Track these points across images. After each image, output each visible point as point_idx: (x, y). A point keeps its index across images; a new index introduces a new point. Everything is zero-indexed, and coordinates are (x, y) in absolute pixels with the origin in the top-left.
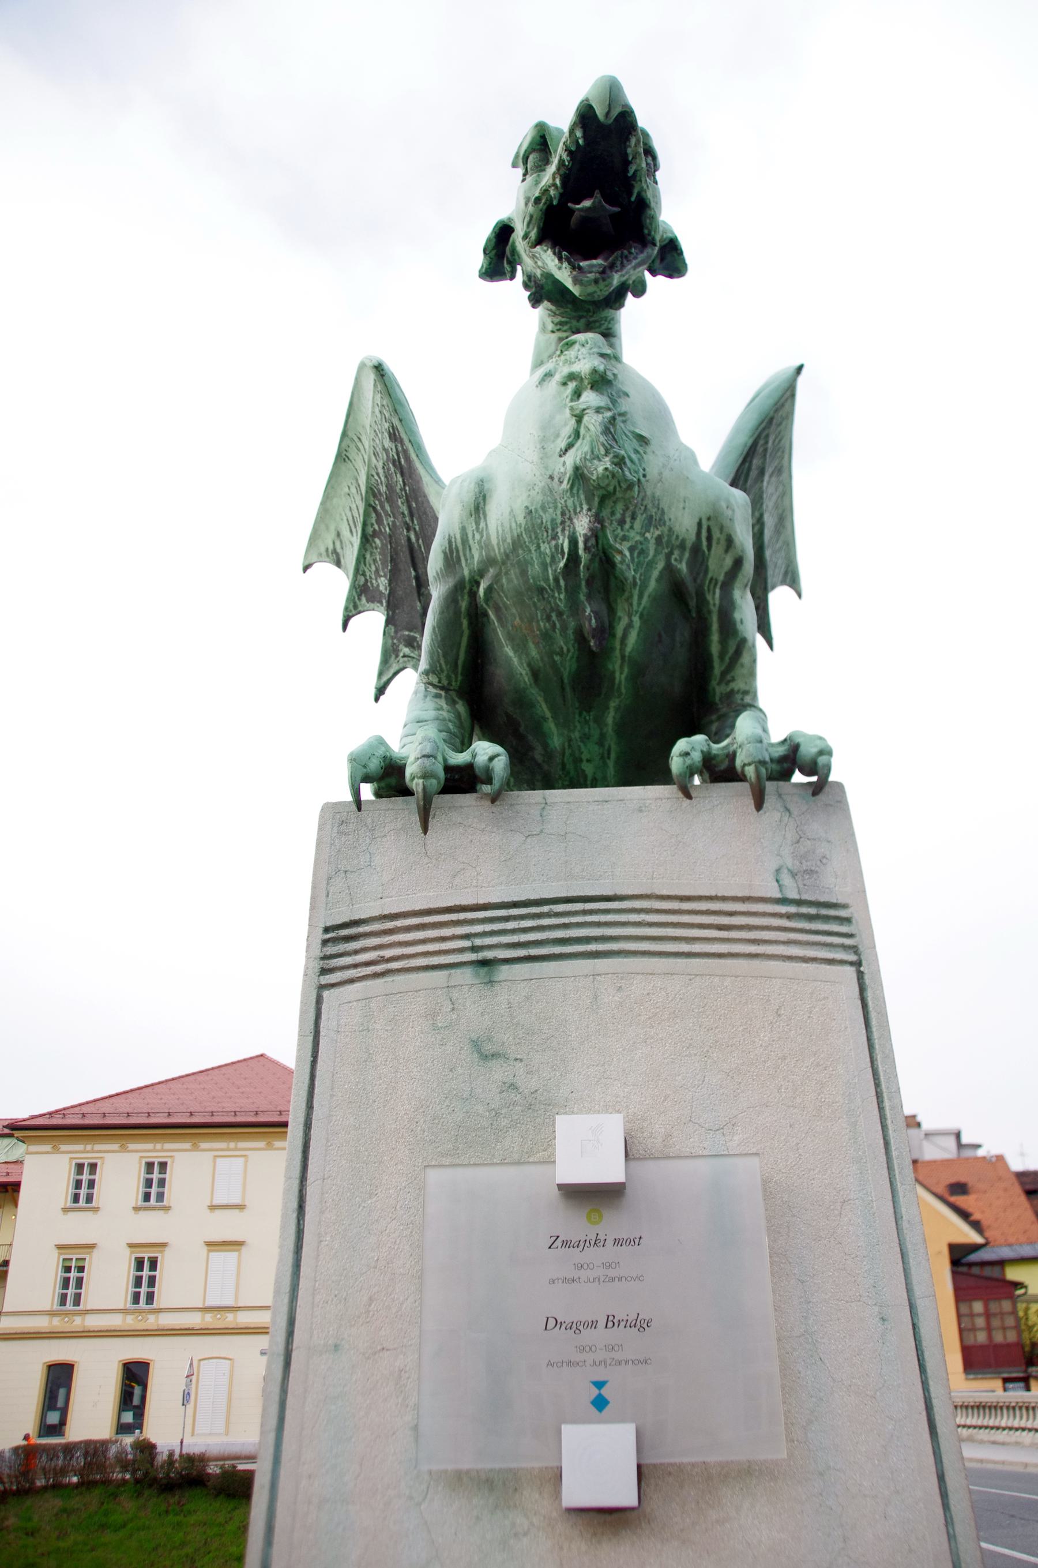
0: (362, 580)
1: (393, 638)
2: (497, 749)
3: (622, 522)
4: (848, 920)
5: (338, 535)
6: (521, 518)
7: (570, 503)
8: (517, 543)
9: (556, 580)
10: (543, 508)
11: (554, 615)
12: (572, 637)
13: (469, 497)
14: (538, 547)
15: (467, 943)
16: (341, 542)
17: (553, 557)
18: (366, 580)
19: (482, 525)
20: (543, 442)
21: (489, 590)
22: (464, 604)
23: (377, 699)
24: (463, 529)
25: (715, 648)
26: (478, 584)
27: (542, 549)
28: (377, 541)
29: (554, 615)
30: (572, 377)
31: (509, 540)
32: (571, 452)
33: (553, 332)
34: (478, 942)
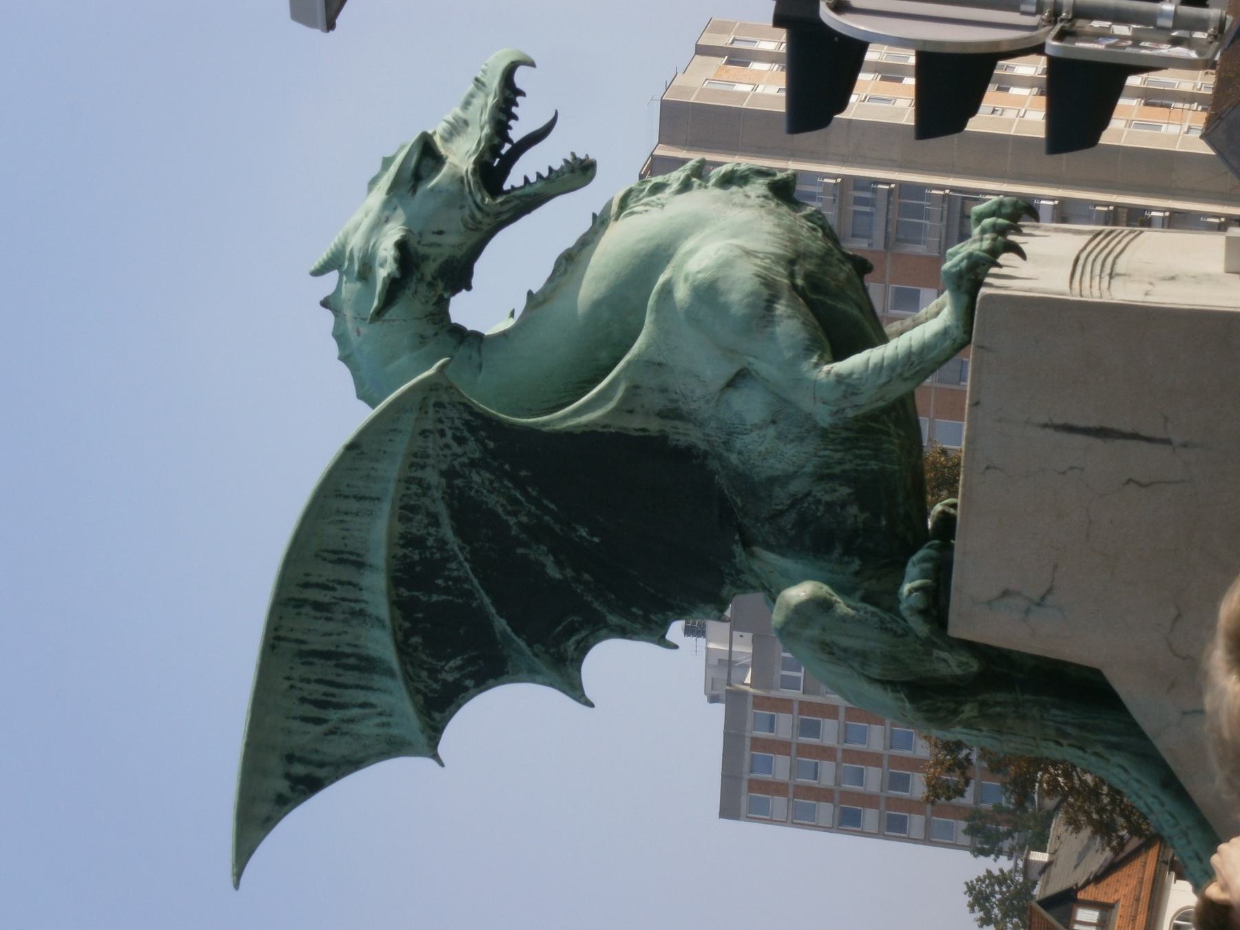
0: (420, 698)
1: (547, 652)
5: (290, 758)
6: (778, 230)
8: (794, 241)
15: (1097, 279)
16: (304, 761)
18: (425, 695)
23: (591, 705)
24: (756, 265)
28: (415, 640)
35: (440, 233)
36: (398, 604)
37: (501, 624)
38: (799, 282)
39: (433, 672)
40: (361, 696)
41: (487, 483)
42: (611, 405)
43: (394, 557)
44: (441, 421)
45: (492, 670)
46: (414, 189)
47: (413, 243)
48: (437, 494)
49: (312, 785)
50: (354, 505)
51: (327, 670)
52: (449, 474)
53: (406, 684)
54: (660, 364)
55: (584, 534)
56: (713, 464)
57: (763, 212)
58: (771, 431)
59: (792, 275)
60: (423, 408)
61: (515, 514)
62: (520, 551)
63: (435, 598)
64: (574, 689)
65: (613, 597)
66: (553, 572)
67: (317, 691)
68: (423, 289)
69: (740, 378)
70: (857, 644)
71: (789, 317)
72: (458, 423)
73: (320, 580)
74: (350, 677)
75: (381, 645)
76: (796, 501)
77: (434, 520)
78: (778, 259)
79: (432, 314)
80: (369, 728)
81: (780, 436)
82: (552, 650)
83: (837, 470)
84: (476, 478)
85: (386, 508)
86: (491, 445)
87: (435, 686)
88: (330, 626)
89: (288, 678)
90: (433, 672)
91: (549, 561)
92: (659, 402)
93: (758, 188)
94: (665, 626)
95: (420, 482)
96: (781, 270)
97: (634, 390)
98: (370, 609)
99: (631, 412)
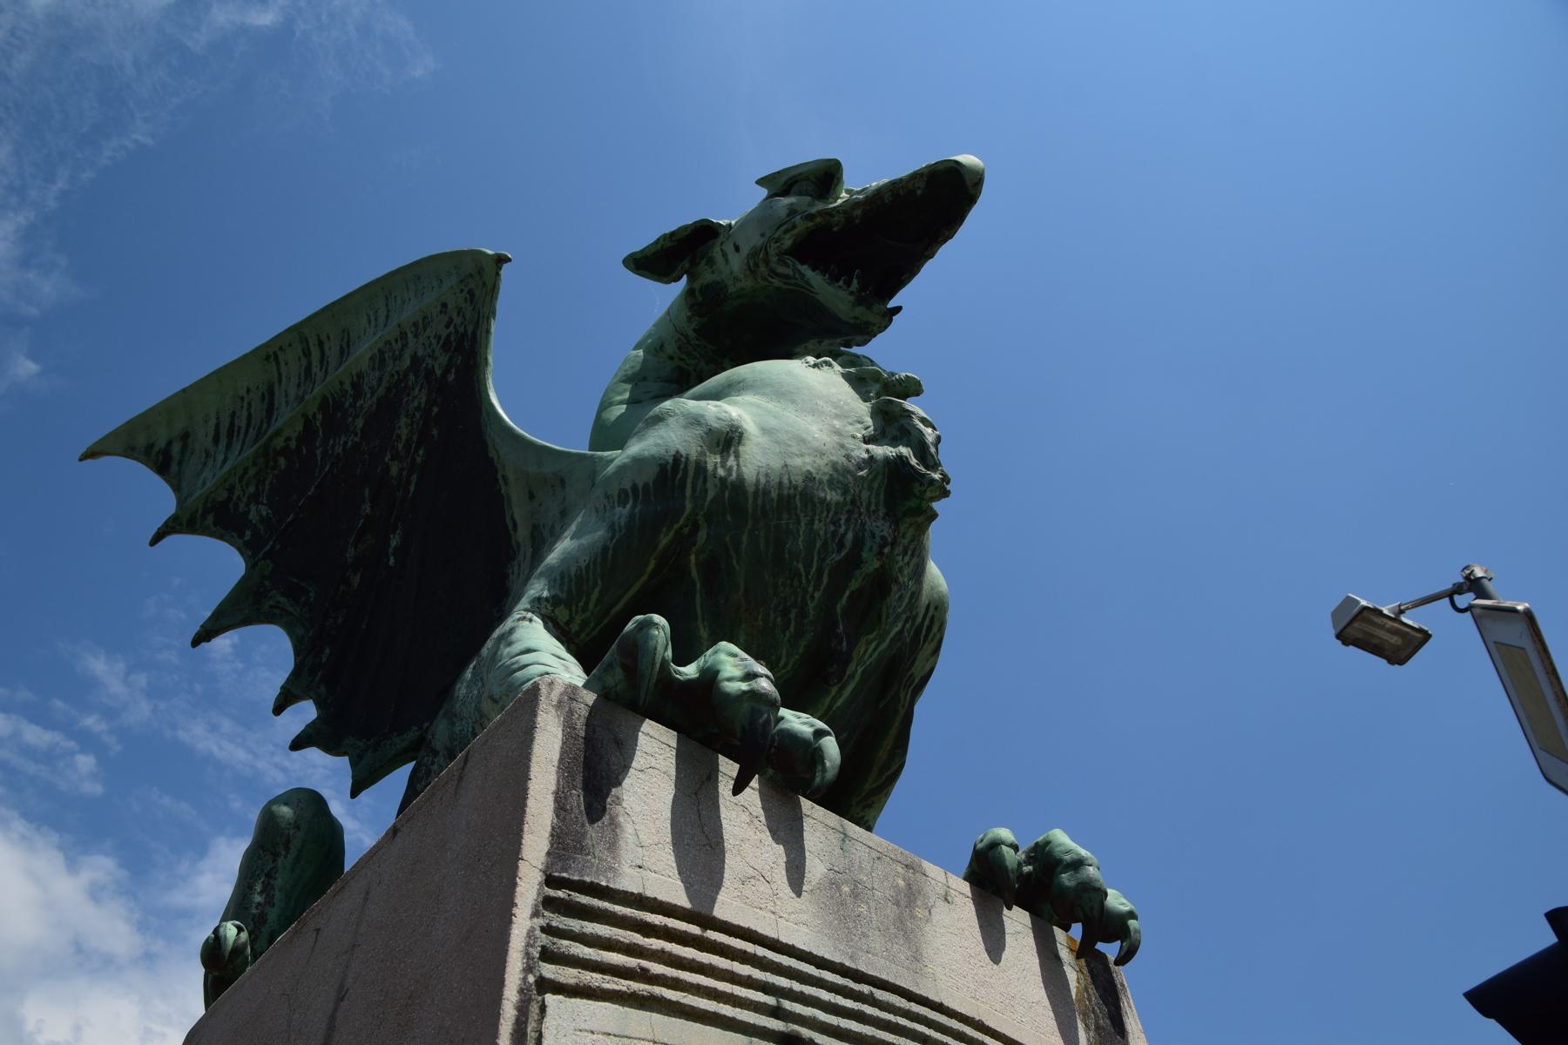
0: (225, 495)
2: (821, 725)
3: (905, 553)
7: (865, 495)
9: (820, 572)
10: (831, 482)
11: (794, 611)
12: (801, 650)
14: (811, 522)
17: (825, 544)
18: (229, 499)
19: (731, 462)
22: (664, 541)
23: (196, 642)
24: (702, 454)
25: (882, 755)
27: (816, 526)
28: (282, 461)
29: (794, 611)
31: (774, 495)
33: (671, 358)
34: (788, 1005)
35: (737, 249)
39: (255, 498)
41: (416, 404)
43: (341, 383)
44: (459, 311)
47: (721, 238)
55: (394, 543)
61: (392, 459)
62: (367, 491)
63: (318, 452)
65: (340, 620)
67: (241, 422)
71: (612, 527)
72: (461, 330)
73: (327, 353)
79: (686, 336)
82: (267, 583)
86: (451, 378)
87: (242, 507)
89: (248, 391)
90: (255, 498)
95: (405, 346)
96: (709, 498)
99: (532, 496)
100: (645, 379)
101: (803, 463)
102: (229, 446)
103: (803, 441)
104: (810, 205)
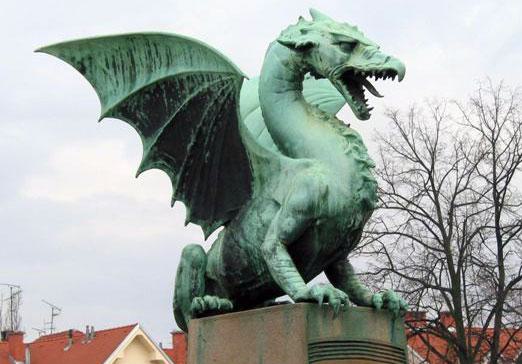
0: (124, 105)
4: (403, 354)
5: (90, 58)
6: (342, 207)
8: (338, 215)
13: (323, 192)
18: (127, 106)
20: (353, 182)
21: (321, 224)
26: (316, 220)
28: (147, 96)
30: (363, 162)
32: (361, 192)
36: (157, 84)
37: (161, 130)
38: (318, 222)
39: (138, 107)
40: (121, 80)
42: (258, 153)
45: (145, 131)
46: (335, 44)
47: (314, 49)
48: (201, 90)
49: (83, 71)
50: (188, 56)
51: (128, 63)
52: (209, 92)
53: (128, 98)
54: (280, 170)
56: (248, 203)
57: (350, 199)
58: (260, 225)
59: (320, 218)
60: (229, 74)
61: (204, 124)
64: (143, 168)
66: (189, 148)
67: (119, 62)
68: (300, 59)
69: (277, 205)
70: (183, 283)
74: (127, 73)
75: (141, 82)
76: (237, 242)
77: (191, 91)
78: (326, 210)
80: (110, 88)
81: (258, 229)
83: (252, 258)
84: (211, 104)
85: (190, 70)
88: (144, 60)
91: (192, 144)
92: (265, 174)
93: (364, 194)
94: (180, 199)
95: (203, 80)
97: (268, 161)
98: (153, 74)
100: (282, 79)
101: (343, 202)
102: (116, 73)
103: (342, 194)
104: (348, 59)
